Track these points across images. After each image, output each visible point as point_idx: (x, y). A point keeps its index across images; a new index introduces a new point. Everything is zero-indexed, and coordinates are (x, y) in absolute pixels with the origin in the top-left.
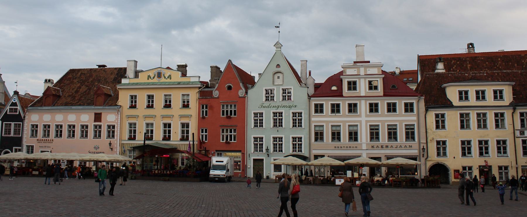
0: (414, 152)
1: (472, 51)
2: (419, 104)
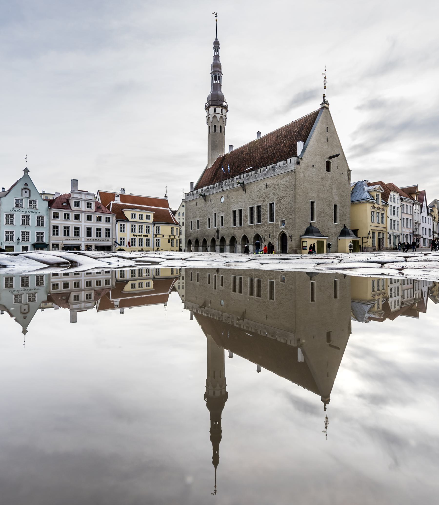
2: (113, 219)
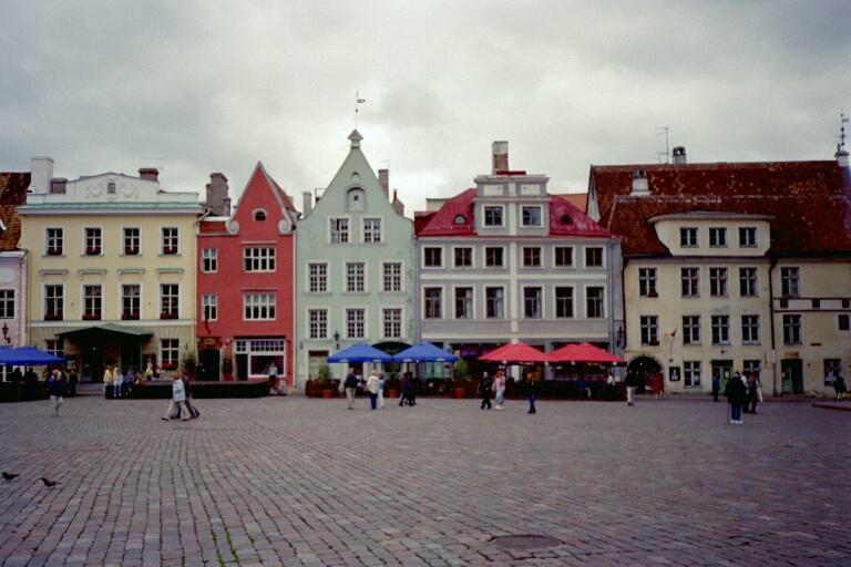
0: (603, 335)
1: (681, 160)
2: (611, 255)
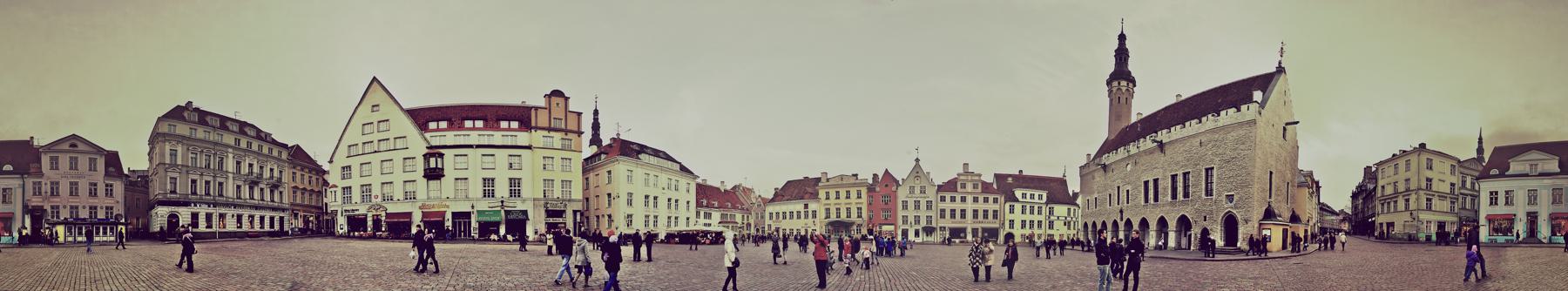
2: (1002, 199)
